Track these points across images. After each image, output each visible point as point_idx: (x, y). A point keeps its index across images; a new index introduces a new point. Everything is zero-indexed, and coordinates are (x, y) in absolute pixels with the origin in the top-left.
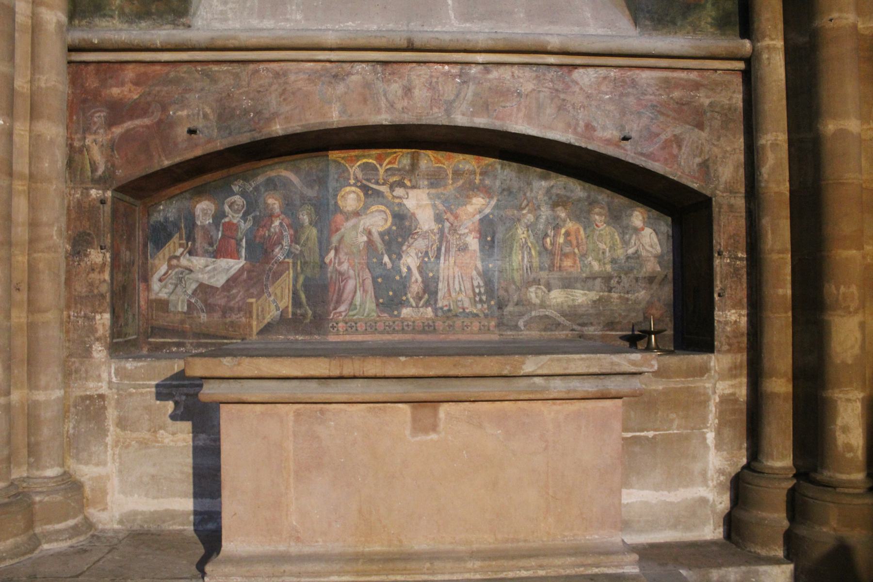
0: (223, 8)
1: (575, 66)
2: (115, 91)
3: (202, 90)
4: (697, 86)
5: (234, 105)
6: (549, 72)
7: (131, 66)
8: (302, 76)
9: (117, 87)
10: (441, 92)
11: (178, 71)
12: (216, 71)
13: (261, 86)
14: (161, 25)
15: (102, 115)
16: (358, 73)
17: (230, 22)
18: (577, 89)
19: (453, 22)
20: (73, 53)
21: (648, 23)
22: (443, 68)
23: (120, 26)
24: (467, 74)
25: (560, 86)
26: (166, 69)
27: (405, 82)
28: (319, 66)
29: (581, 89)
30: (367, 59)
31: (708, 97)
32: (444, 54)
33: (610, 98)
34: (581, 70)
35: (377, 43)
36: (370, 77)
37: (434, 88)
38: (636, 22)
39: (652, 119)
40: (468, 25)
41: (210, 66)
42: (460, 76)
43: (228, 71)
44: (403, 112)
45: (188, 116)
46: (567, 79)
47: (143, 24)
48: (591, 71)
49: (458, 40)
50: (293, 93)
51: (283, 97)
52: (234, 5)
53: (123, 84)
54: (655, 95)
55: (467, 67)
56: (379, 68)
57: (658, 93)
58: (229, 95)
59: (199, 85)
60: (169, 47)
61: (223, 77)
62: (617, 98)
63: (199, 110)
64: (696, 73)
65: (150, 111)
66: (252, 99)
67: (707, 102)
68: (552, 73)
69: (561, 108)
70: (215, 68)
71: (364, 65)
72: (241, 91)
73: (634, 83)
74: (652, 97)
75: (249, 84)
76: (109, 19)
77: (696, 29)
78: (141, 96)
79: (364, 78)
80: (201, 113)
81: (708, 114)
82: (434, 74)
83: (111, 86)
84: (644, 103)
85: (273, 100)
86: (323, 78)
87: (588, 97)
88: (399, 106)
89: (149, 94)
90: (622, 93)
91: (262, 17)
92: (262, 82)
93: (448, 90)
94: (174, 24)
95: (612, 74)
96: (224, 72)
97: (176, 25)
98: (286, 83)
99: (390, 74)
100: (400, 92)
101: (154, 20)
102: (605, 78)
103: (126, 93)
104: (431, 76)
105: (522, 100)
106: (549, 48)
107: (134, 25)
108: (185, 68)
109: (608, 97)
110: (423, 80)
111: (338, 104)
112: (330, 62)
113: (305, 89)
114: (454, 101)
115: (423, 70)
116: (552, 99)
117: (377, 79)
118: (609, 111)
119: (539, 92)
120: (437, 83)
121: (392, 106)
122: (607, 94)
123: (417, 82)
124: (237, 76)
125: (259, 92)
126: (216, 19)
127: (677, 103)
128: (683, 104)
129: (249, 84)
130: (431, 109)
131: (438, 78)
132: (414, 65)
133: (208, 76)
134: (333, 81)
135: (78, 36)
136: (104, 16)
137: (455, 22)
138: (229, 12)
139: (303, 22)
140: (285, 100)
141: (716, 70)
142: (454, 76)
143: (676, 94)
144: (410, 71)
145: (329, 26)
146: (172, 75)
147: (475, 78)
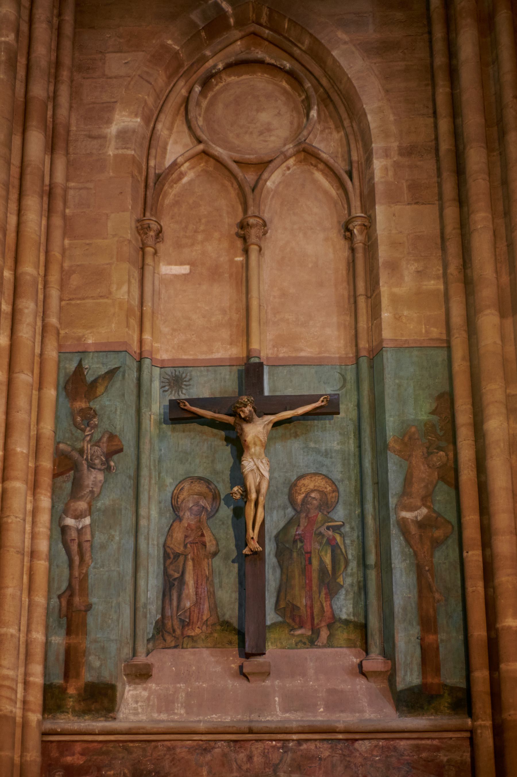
0: (135, 705)
1: (357, 740)
2: (69, 759)
3: (123, 758)
4: (438, 749)
5: (142, 768)
6: (339, 744)
7: (78, 744)
8: (184, 749)
9: (71, 756)
10: (271, 758)
11: (108, 747)
12: (131, 747)
13: (159, 756)
14: (98, 718)
15: (61, 773)
16: (219, 747)
17: (140, 715)
18: (357, 754)
19: (278, 713)
20: (44, 736)
21: (405, 709)
22: (272, 743)
23: (72, 718)
24: (287, 747)
25: (346, 752)
26: (100, 745)
27: (248, 753)
28: (195, 743)
29: (360, 754)
30: (224, 739)
31: (445, 756)
32: (272, 735)
33: (379, 759)
34: (360, 742)
35: (230, 730)
36: (226, 750)
37: (266, 756)
38: (397, 709)
39: (408, 772)
40: (287, 715)
41: (128, 743)
42: (282, 748)
43: (139, 746)
44: (247, 772)
45: (114, 774)
46: (351, 748)
47: (87, 717)
48: (367, 742)
49: (280, 728)
50: (179, 760)
51: (173, 763)
52: (142, 704)
53: (73, 754)
54: (410, 756)
55: (287, 743)
56: (232, 744)
57: (411, 754)
58: (139, 761)
59: (121, 755)
60: (103, 733)
61: (135, 750)
62: (384, 758)
63: (121, 771)
64: (437, 740)
65: (91, 771)
66: (153, 764)
67: (445, 759)
68: (340, 745)
69: (347, 767)
70: (131, 745)
71: (223, 742)
72: (147, 759)
73: (395, 749)
74: (408, 758)
75: (152, 754)
76: (66, 714)
77: (437, 711)
78: (84, 762)
79: (222, 750)
80: (122, 773)
81: (446, 767)
82: (266, 747)
83: (67, 756)
84: (402, 761)
85: (167, 764)
86: (197, 751)
87: (365, 759)
88: (244, 767)
89: (90, 760)
90: (387, 756)
91: (160, 712)
92: (159, 753)
93: (275, 757)
94: (105, 717)
95: (381, 743)
96: (136, 747)
97: (107, 719)
98: (174, 754)
99: (239, 748)
100: (245, 759)
101: (93, 714)
102: (376, 746)
103: (75, 760)
104: (264, 749)
105: (322, 762)
106: (338, 730)
107: (81, 718)
108: (112, 745)
109: (378, 758)
110: (259, 751)
111: (207, 767)
112: (202, 741)
113: (186, 757)
114: (279, 764)
115: (259, 745)
116: (341, 761)
117: (231, 751)
118: (379, 768)
119: (333, 756)
120: (268, 752)
121: (240, 768)
122: (377, 757)
123: (255, 753)
124: (144, 750)
125: (158, 760)
126: (131, 713)
127: (425, 760)
128: (429, 761)
129: (152, 754)
130: (265, 769)
131: (268, 750)
132: (254, 742)
133: (126, 749)
134: (204, 752)
135: (48, 725)
136: (63, 712)
137: (279, 713)
138: (139, 708)
139: (185, 715)
140: (174, 764)
141: (451, 738)
142: (279, 748)
143: (424, 755)
144: (251, 745)
145: (201, 718)
146: (104, 749)
147: (292, 749)
